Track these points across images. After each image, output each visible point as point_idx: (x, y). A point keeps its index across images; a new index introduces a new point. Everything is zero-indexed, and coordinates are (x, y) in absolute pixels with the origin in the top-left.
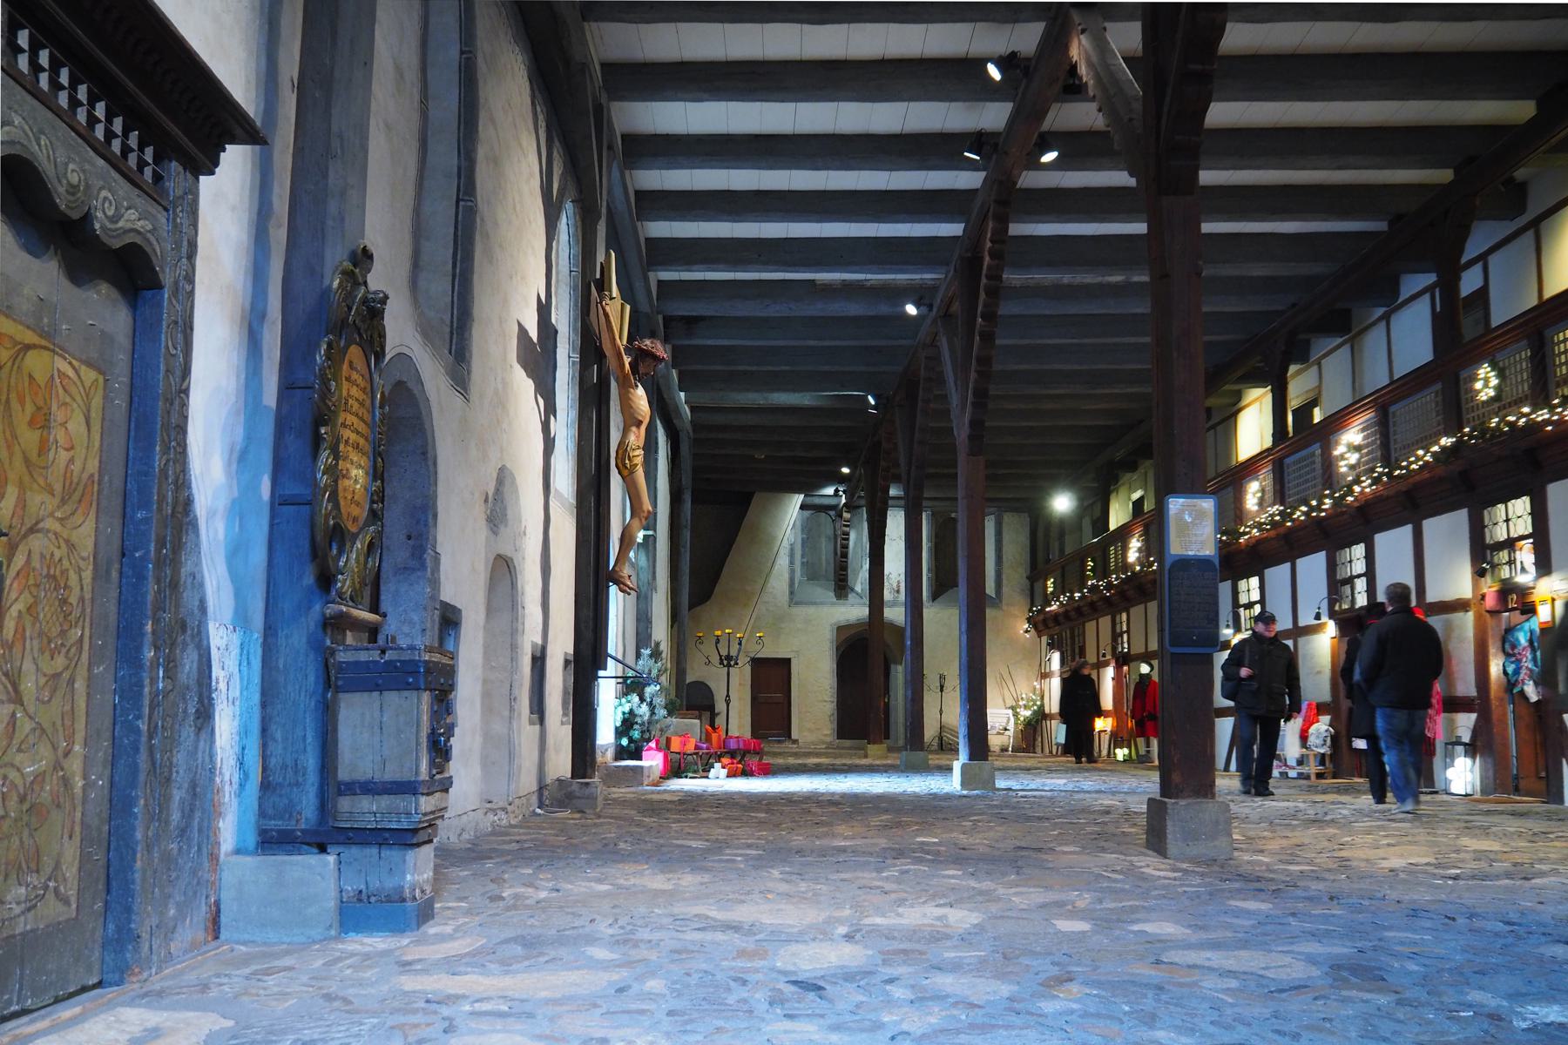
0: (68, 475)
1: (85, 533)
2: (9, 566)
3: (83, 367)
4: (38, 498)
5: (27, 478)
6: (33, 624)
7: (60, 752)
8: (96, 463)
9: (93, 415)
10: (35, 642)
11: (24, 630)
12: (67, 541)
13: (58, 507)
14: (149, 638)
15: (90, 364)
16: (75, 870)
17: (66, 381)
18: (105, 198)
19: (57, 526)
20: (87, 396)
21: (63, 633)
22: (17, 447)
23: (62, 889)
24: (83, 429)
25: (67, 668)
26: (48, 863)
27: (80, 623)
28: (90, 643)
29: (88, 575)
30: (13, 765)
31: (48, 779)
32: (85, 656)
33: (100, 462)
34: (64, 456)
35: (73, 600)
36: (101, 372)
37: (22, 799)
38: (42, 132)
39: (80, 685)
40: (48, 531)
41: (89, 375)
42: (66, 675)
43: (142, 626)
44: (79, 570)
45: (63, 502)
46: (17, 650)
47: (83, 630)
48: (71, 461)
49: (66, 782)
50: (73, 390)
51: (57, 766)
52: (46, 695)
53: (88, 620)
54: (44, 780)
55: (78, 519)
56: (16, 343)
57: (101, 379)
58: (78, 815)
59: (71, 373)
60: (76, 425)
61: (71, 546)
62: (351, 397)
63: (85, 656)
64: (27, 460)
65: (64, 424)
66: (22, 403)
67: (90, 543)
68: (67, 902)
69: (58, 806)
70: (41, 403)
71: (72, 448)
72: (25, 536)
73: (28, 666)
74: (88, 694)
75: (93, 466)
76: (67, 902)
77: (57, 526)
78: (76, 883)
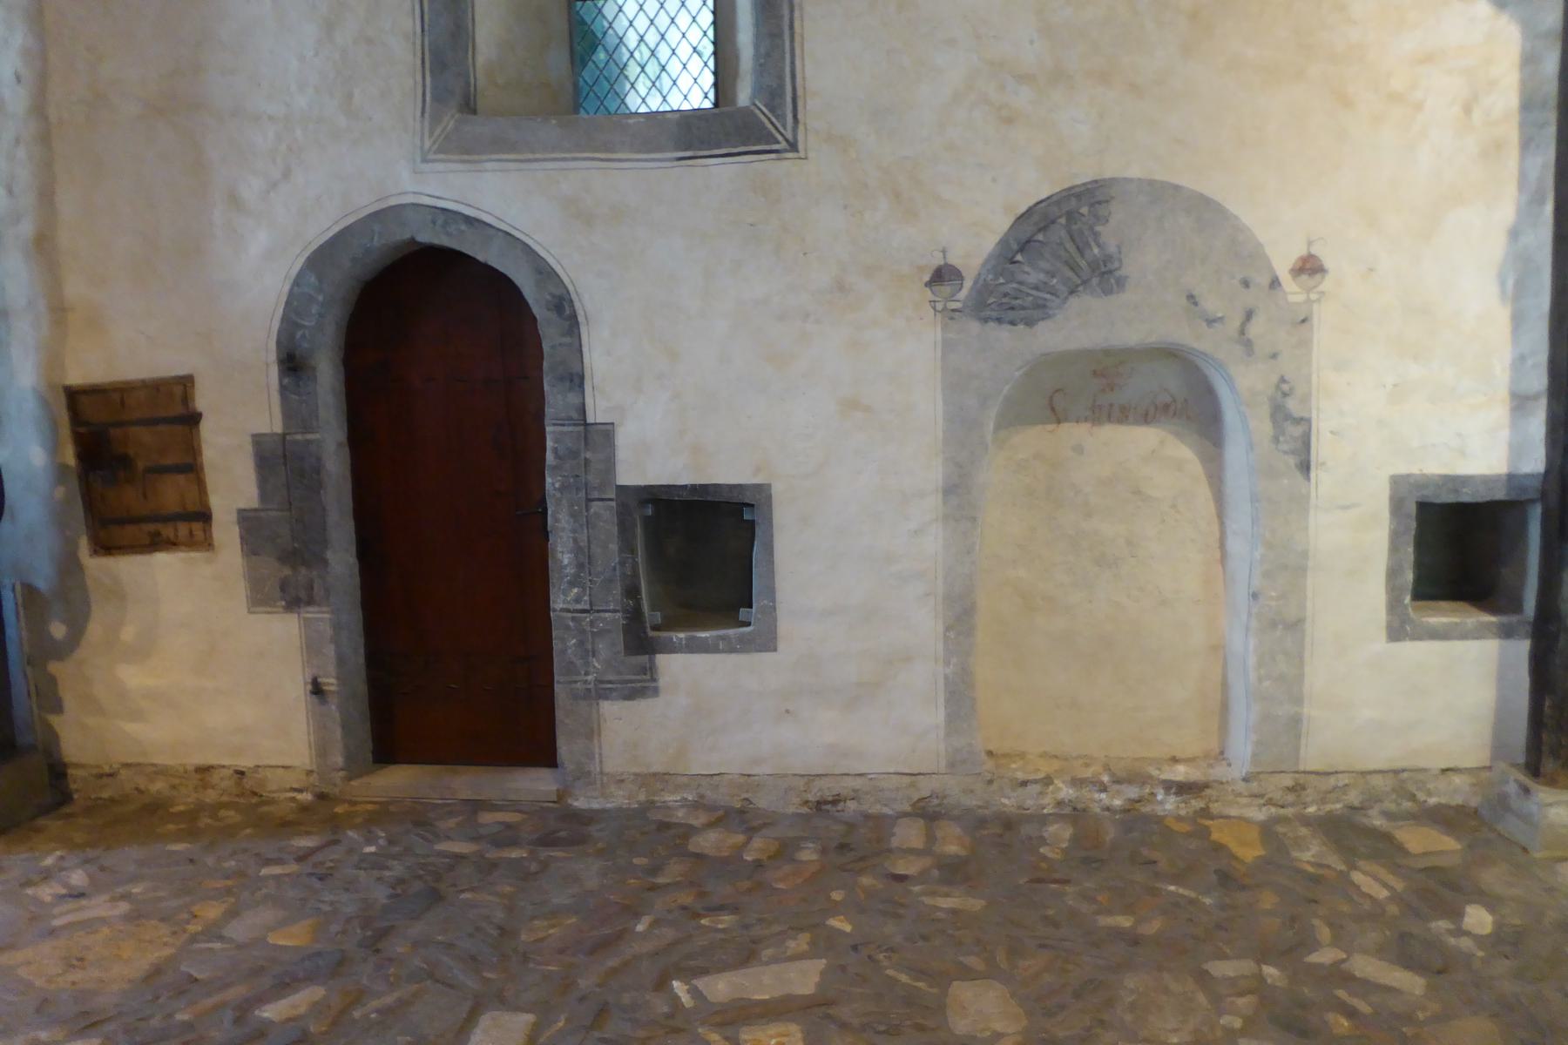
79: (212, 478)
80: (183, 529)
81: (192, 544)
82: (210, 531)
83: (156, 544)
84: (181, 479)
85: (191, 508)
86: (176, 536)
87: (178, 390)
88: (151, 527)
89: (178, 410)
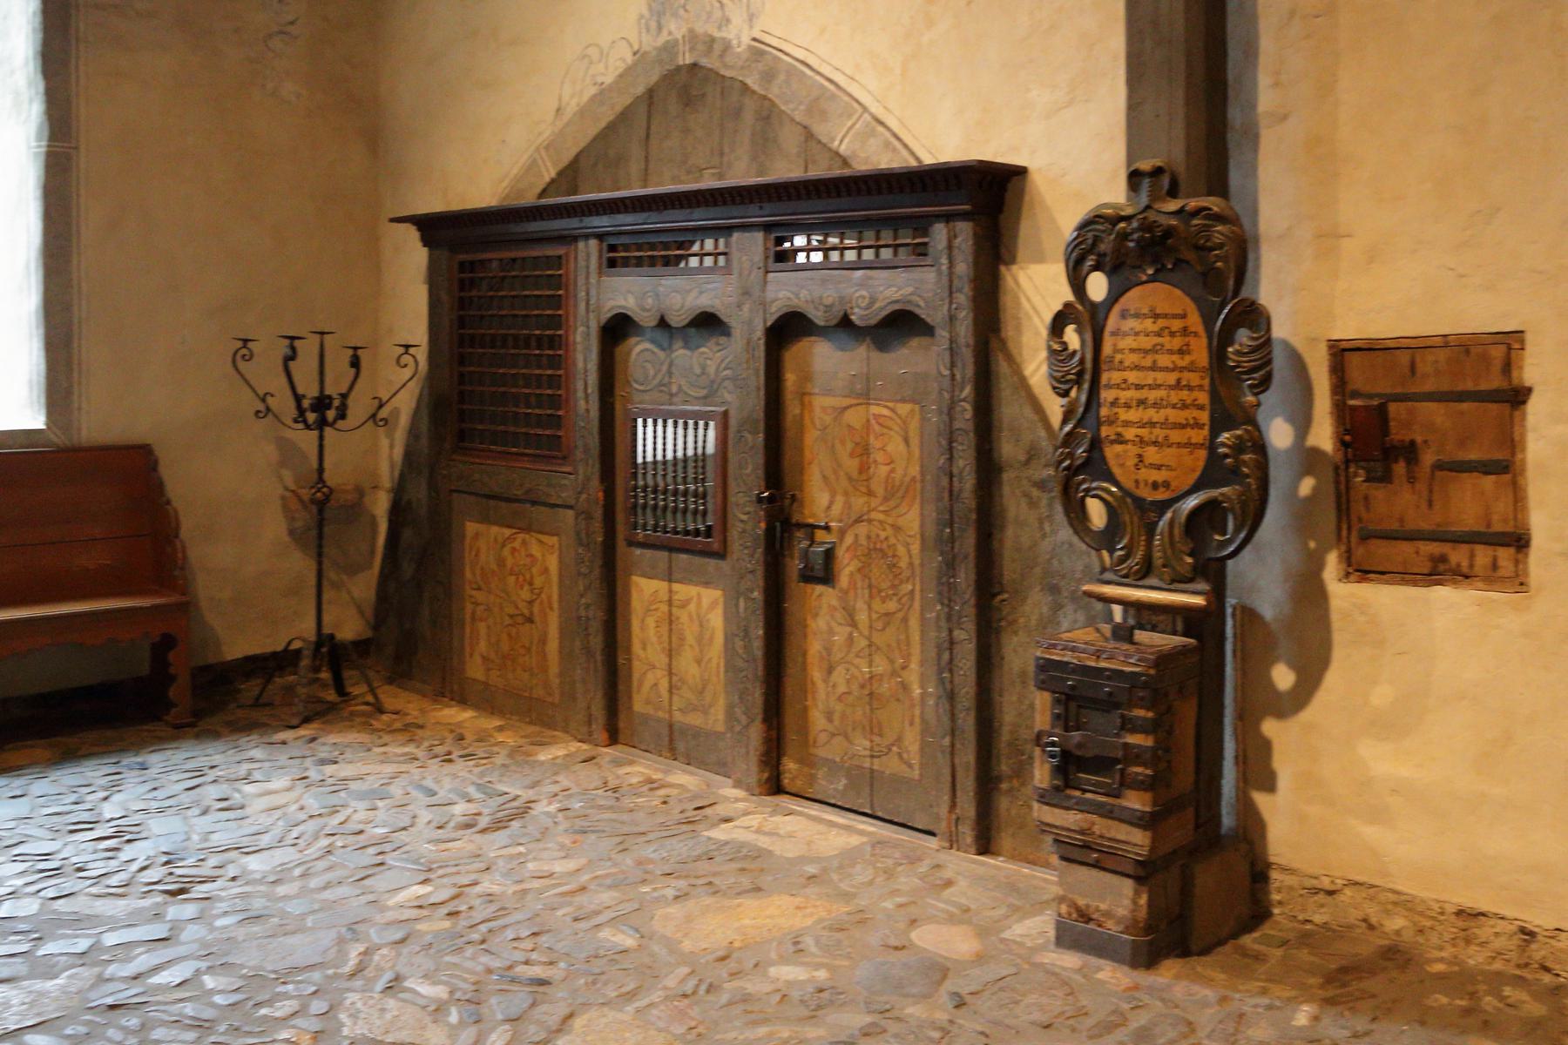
3: (899, 405)
11: (855, 584)
13: (881, 504)
15: (903, 401)
17: (881, 421)
19: (881, 517)
20: (904, 422)
21: (894, 587)
24: (902, 447)
25: (900, 610)
27: (911, 581)
29: (916, 548)
30: (853, 664)
32: (917, 605)
34: (883, 470)
35: (903, 564)
36: (913, 401)
37: (862, 687)
39: (914, 623)
40: (874, 520)
41: (903, 409)
42: (900, 615)
44: (907, 545)
45: (886, 499)
46: (851, 594)
47: (914, 585)
48: (892, 471)
49: (905, 687)
50: (890, 423)
51: (894, 673)
52: (879, 625)
53: (918, 578)
54: (881, 680)
55: (902, 510)
56: (834, 408)
57: (917, 407)
58: (917, 712)
59: (885, 412)
60: (896, 446)
61: (897, 528)
62: (1121, 351)
64: (850, 479)
66: (843, 442)
68: (910, 766)
69: (898, 700)
70: (858, 439)
71: (892, 462)
72: (852, 525)
73: (860, 605)
74: (922, 631)
75: (915, 470)
76: (910, 766)
77: (881, 517)
80: (1483, 555)
81: (1492, 578)
82: (1526, 563)
83: (1437, 573)
84: (1488, 482)
85: (1498, 527)
86: (1471, 566)
87: (1497, 353)
89: (1494, 382)
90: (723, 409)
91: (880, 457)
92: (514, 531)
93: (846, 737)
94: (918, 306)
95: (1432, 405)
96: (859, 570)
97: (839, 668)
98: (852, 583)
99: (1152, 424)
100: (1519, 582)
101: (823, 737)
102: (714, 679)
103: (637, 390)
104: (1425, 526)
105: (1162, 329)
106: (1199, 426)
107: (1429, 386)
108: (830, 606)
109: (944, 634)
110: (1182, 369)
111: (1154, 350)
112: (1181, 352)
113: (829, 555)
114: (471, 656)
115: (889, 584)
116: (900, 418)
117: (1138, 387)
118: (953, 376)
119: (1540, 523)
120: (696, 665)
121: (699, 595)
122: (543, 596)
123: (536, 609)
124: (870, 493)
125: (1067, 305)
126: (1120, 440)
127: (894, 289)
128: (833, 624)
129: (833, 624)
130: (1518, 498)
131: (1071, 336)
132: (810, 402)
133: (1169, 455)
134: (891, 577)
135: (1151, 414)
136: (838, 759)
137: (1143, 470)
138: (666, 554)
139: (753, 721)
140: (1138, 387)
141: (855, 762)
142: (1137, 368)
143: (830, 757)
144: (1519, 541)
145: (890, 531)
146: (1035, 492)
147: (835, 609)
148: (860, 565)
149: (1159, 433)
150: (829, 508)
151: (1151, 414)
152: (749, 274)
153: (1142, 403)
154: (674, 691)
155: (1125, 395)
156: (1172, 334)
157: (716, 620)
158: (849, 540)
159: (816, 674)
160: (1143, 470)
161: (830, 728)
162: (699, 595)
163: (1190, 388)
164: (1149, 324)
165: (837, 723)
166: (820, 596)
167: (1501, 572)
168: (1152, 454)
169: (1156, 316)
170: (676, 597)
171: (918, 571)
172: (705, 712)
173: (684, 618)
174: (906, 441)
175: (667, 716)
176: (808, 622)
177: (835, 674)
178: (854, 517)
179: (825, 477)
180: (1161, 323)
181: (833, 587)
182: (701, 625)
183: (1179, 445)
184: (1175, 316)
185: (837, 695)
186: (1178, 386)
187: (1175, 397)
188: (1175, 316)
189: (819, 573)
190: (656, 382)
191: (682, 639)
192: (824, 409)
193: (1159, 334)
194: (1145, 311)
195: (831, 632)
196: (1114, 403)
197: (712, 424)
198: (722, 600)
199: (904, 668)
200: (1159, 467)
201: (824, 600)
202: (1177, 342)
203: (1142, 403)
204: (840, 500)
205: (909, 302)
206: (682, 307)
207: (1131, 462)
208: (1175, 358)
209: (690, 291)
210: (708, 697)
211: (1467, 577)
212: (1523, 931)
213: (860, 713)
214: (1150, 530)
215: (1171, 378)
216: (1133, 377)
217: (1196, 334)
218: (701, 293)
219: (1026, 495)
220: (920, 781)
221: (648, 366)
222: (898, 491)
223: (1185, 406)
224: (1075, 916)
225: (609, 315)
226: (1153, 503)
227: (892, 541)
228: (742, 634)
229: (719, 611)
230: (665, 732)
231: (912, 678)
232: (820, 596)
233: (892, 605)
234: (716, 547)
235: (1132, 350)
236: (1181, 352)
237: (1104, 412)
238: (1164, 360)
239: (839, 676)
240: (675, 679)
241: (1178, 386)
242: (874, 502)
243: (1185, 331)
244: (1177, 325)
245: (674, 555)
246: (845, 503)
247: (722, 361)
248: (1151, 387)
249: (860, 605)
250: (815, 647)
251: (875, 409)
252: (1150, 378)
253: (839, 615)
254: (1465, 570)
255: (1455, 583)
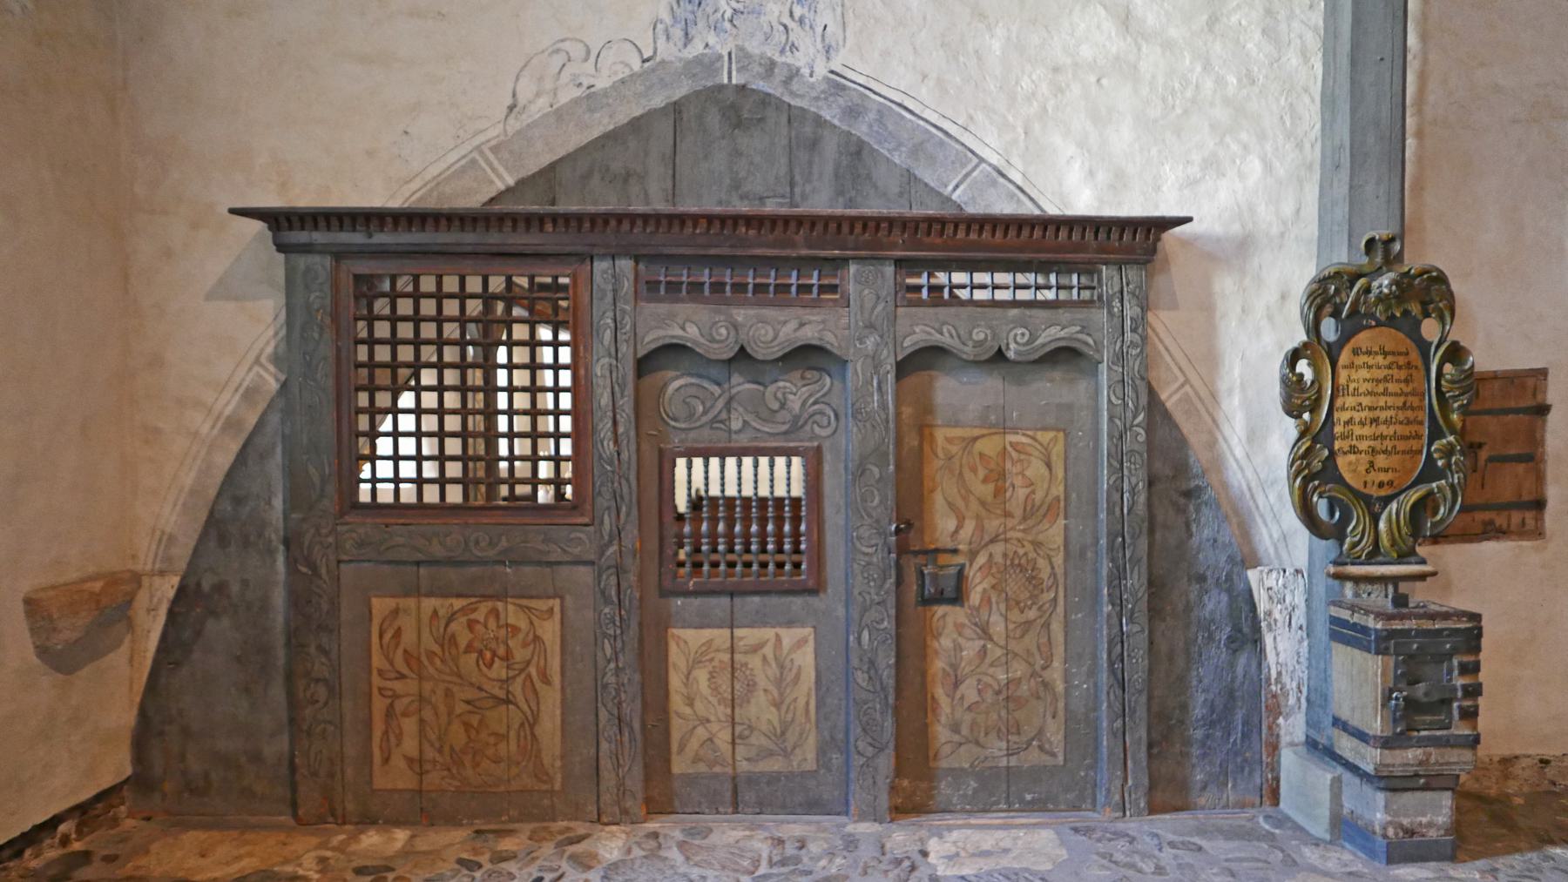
0: (1029, 503)
1: (1054, 533)
2: (971, 565)
4: (996, 523)
5: (984, 513)
6: (999, 595)
7: (1037, 668)
8: (1061, 488)
9: (1054, 458)
10: (1003, 607)
12: (1032, 542)
13: (1020, 523)
14: (1106, 598)
15: (1045, 429)
16: (1060, 736)
18: (1016, 335)
19: (1020, 535)
21: (1032, 597)
22: (972, 498)
23: (1047, 746)
24: (1044, 471)
25: (1041, 617)
26: (1029, 731)
27: (1054, 588)
28: (1065, 601)
29: (1059, 560)
31: (1024, 682)
32: (1060, 609)
33: (1066, 486)
34: (1022, 493)
35: (1045, 574)
36: (1058, 430)
38: (944, 323)
39: (1057, 627)
43: (1102, 590)
45: (1025, 519)
47: (1057, 593)
49: (1046, 685)
50: (1029, 449)
51: (1034, 675)
56: (964, 439)
58: (1061, 705)
59: (1024, 440)
60: (1036, 469)
61: (1037, 545)
63: (1060, 609)
64: (983, 503)
65: (1022, 474)
66: (974, 470)
67: (1060, 540)
68: (1054, 755)
69: (1038, 698)
70: (992, 465)
73: (995, 618)
75: (1059, 490)
78: (1062, 744)
79: (1551, 471)
80: (1516, 517)
81: (1522, 533)
86: (1509, 525)
88: (1487, 515)
89: (1528, 402)
90: (816, 444)
91: (1018, 481)
92: (473, 600)
93: (977, 743)
94: (1087, 344)
95: (1487, 418)
96: (993, 587)
97: (967, 682)
98: (986, 599)
99: (1383, 437)
100: (1538, 533)
101: (946, 749)
102: (801, 718)
103: (674, 427)
104: (1478, 501)
105: (1392, 363)
106: (1418, 437)
107: (1488, 405)
108: (955, 625)
109: (1116, 630)
110: (1407, 395)
111: (1386, 380)
112: (1407, 381)
113: (960, 575)
114: (386, 760)
115: (1028, 595)
116: (1041, 444)
117: (1371, 408)
118: (1125, 405)
119: (1553, 493)
120: (773, 709)
121: (777, 635)
122: (533, 670)
123: (517, 688)
124: (1007, 514)
125: (1305, 345)
126: (1353, 450)
127: (1059, 328)
128: (960, 640)
129: (960, 640)
130: (1540, 478)
131: (1303, 367)
132: (931, 435)
133: (1394, 461)
134: (1031, 588)
135: (1383, 429)
136: (966, 766)
137: (1373, 473)
138: (725, 601)
139: (881, 750)
140: (1371, 408)
141: (987, 764)
142: (1370, 393)
143: (957, 766)
144: (1539, 505)
145: (1029, 547)
146: (1182, 501)
147: (963, 625)
148: (994, 581)
149: (1388, 444)
150: (956, 532)
151: (1383, 429)
152: (874, 307)
153: (1375, 421)
154: (738, 741)
155: (1357, 416)
156: (1399, 368)
157: (806, 659)
158: (981, 559)
159: (940, 692)
160: (1373, 473)
161: (956, 738)
162: (777, 635)
163: (1412, 408)
164: (1380, 359)
165: (965, 731)
166: (944, 616)
167: (1527, 528)
168: (1381, 461)
169: (1385, 354)
170: (741, 643)
171: (1061, 581)
172: (786, 754)
173: (755, 662)
174: (1049, 465)
175: (729, 770)
176: (929, 643)
177: (963, 687)
178: (987, 538)
179: (951, 505)
180: (1390, 359)
181: (962, 606)
182: (782, 667)
183: (1404, 452)
184: (1400, 354)
185: (966, 705)
186: (1404, 407)
187: (1401, 416)
188: (1400, 354)
189: (949, 592)
190: (705, 419)
191: (751, 686)
192: (949, 440)
193: (1389, 367)
194: (1376, 349)
195: (958, 648)
196: (1349, 422)
197: (796, 461)
198: (812, 637)
199: (1044, 668)
200: (1386, 470)
201: (950, 620)
202: (1403, 374)
203: (1375, 421)
204: (969, 527)
205: (1079, 340)
206: (775, 338)
207: (1362, 469)
208: (1403, 385)
209: (785, 322)
210: (791, 737)
211: (1504, 533)
212: (1542, 761)
213: (995, 717)
214: (1375, 520)
215: (1399, 401)
216: (1366, 401)
217: (1416, 368)
218: (802, 325)
219: (1174, 504)
220: (1064, 765)
221: (694, 402)
222: (1039, 507)
223: (1409, 422)
224: (1401, 834)
225: (653, 346)
226: (1379, 499)
227: (1032, 555)
228: (865, 668)
229: (810, 648)
230: (728, 786)
231: (1055, 676)
232: (944, 616)
233: (1032, 614)
234: (811, 583)
235: (1365, 380)
236: (1407, 381)
237: (1338, 429)
238: (1392, 387)
239: (969, 691)
240: (738, 729)
241: (1404, 407)
242: (1010, 523)
243: (1409, 365)
244: (1402, 360)
245: (737, 600)
246: (977, 525)
247: (810, 396)
248: (1382, 408)
249: (995, 618)
250: (939, 665)
251: (1011, 438)
252: (1382, 401)
253: (968, 632)
254: (1505, 526)
255: (1498, 538)
